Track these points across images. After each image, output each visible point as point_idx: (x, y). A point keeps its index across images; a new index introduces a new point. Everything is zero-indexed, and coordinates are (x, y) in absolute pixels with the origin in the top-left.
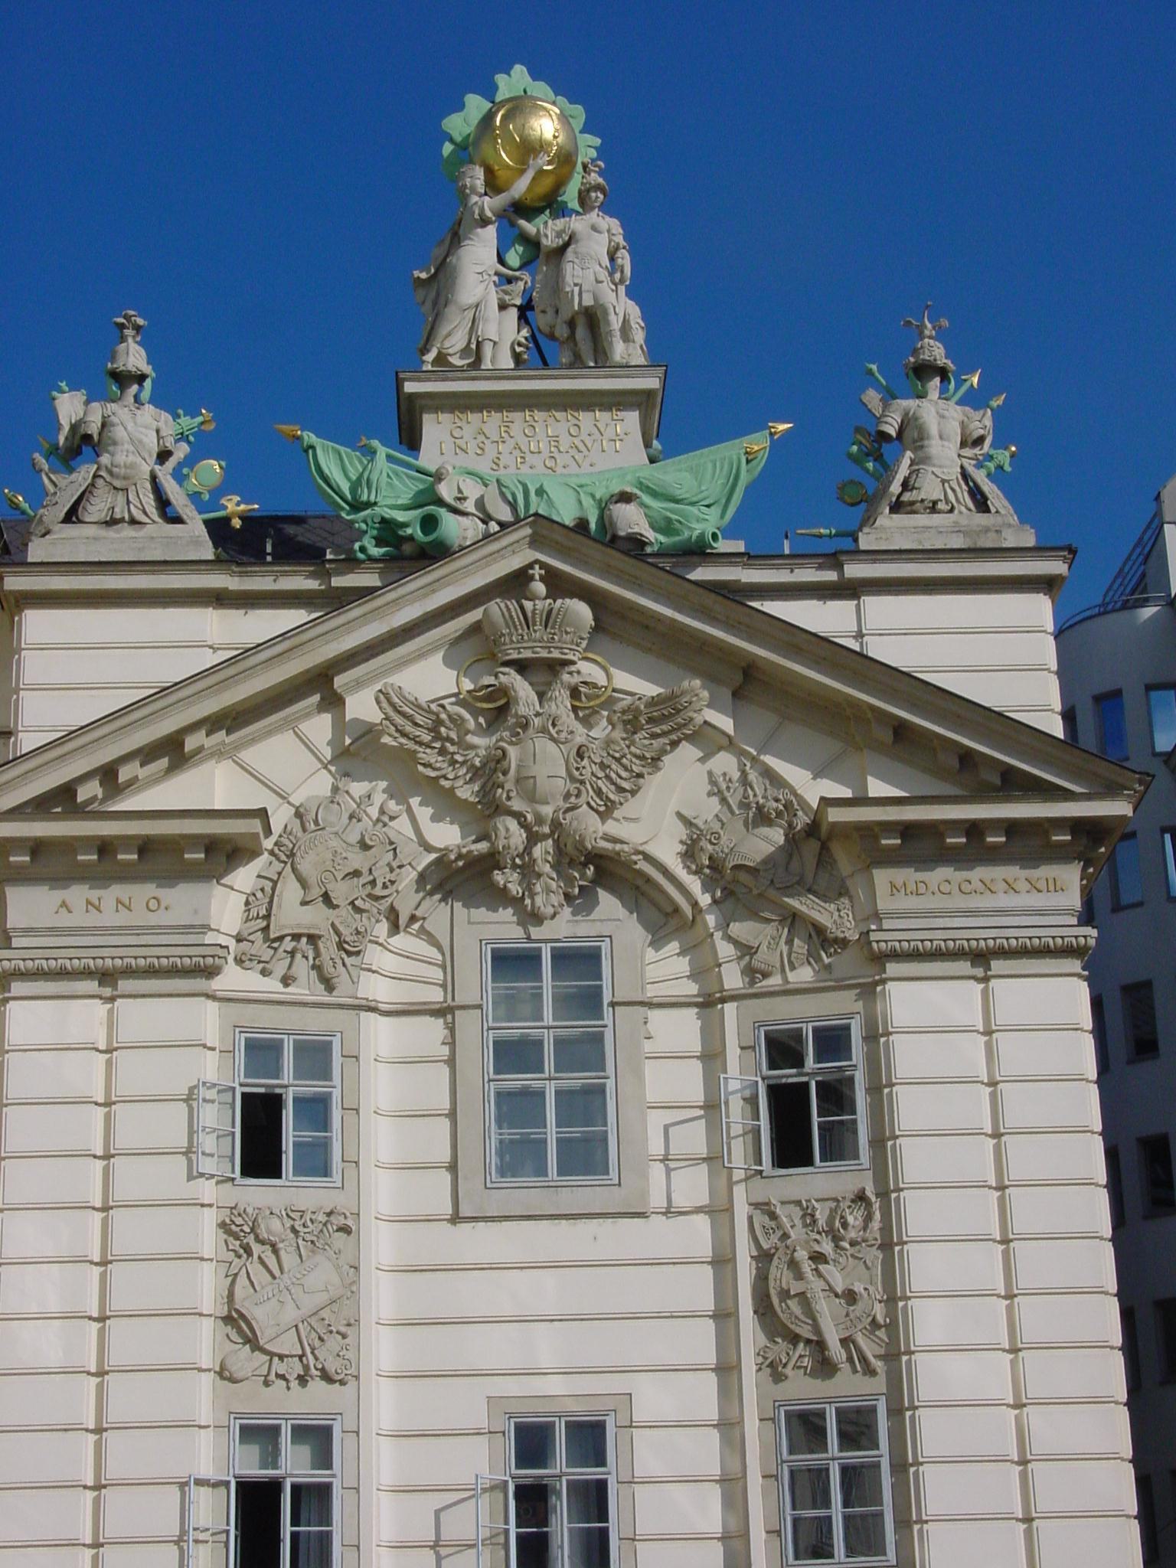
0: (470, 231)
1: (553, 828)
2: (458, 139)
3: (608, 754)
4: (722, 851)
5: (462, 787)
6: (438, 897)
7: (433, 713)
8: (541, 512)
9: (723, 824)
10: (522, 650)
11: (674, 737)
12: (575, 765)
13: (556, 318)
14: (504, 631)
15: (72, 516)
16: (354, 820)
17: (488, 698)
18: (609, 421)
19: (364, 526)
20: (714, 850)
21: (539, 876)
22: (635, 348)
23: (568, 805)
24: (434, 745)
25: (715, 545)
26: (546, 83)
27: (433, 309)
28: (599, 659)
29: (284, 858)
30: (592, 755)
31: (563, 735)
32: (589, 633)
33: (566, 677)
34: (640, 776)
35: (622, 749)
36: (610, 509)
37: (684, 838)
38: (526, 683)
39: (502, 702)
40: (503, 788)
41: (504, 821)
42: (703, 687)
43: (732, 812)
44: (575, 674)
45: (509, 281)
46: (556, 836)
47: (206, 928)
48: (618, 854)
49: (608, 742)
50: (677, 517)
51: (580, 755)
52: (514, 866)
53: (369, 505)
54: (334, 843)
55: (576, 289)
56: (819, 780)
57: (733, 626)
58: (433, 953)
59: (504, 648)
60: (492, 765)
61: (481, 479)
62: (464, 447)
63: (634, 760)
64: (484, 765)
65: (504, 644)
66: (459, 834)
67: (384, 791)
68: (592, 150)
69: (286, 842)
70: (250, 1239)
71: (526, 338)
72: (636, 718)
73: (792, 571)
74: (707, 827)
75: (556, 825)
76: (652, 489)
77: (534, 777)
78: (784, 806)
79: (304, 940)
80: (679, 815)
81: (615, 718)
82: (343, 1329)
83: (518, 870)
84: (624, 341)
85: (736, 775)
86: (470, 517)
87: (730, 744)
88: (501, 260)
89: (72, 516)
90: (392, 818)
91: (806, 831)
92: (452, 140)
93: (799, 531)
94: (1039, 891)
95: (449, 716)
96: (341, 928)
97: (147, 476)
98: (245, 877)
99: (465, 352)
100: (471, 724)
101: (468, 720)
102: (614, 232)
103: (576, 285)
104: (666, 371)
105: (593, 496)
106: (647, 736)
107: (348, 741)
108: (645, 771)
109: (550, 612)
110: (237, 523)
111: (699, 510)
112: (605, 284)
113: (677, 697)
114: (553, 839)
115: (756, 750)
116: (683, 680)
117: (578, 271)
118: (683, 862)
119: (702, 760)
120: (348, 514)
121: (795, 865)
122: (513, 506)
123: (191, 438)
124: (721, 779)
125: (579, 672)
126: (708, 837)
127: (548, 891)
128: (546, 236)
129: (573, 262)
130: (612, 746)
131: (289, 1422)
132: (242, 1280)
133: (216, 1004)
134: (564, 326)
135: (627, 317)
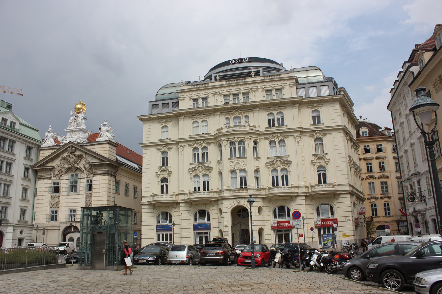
15: (45, 143)
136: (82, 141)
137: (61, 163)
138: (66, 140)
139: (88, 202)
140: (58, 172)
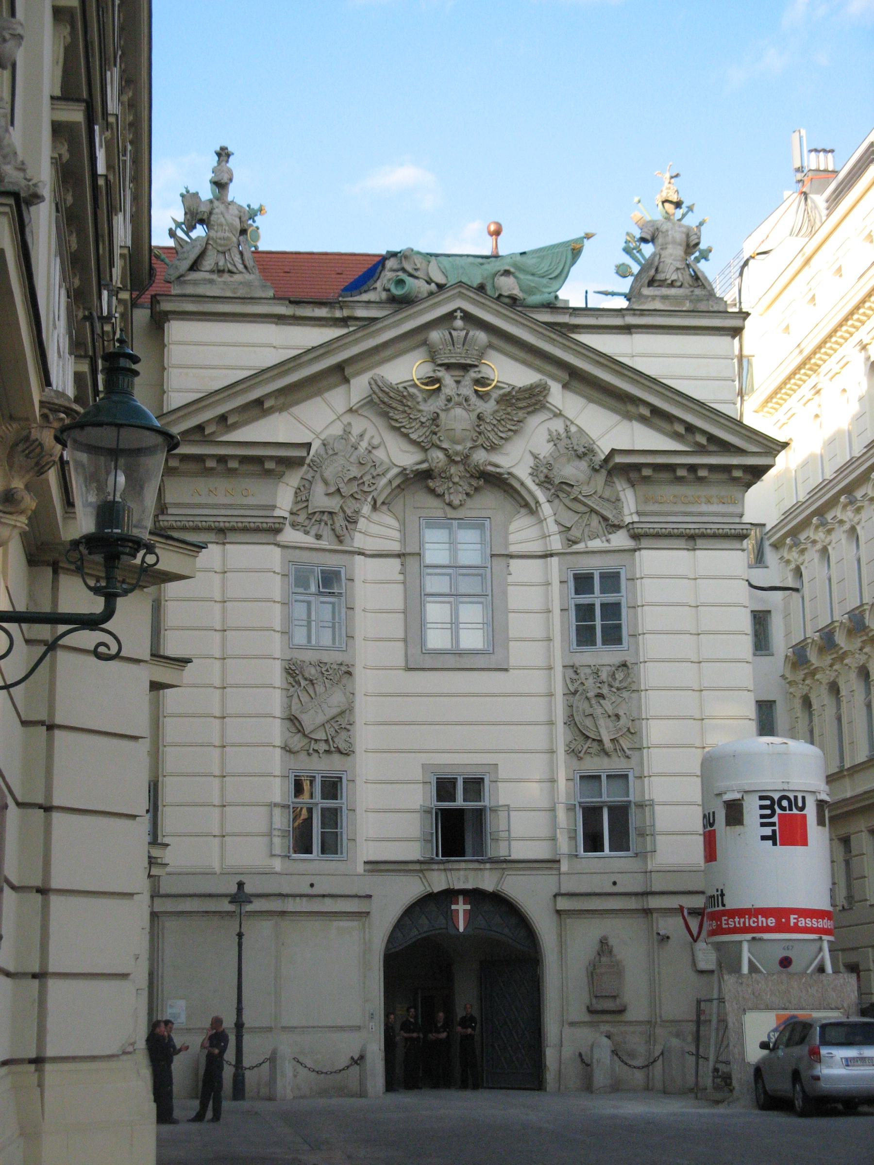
33: (473, 374)
39: (437, 386)
47: (274, 507)
48: (497, 473)
58: (395, 523)
60: (431, 422)
65: (440, 354)
70: (300, 678)
79: (326, 514)
82: (348, 727)
89: (195, 266)
94: (724, 503)
96: (346, 509)
98: (293, 479)
100: (420, 399)
131: (320, 775)
132: (295, 700)
133: (279, 549)
136: (530, 291)
137: (356, 431)
138: (404, 270)
139: (602, 722)
140: (328, 495)
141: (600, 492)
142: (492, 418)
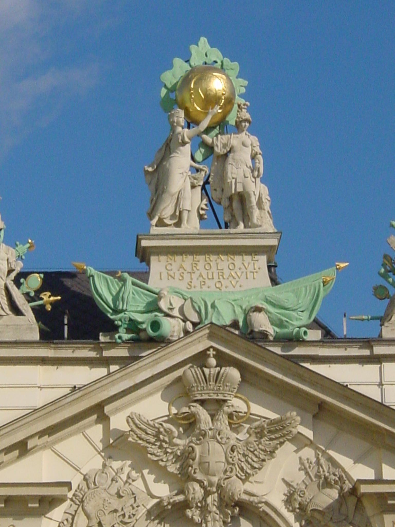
0: (177, 148)
1: (218, 488)
2: (169, 86)
3: (248, 449)
4: (306, 501)
5: (170, 465)
6: (157, 521)
7: (156, 428)
8: (214, 321)
9: (307, 486)
10: (203, 395)
11: (281, 440)
12: (230, 455)
13: (223, 194)
14: (194, 385)
16: (114, 482)
17: (184, 419)
18: (250, 261)
19: (120, 323)
20: (301, 500)
21: (210, 512)
22: (265, 213)
23: (226, 477)
24: (156, 444)
25: (305, 337)
26: (218, 49)
27: (156, 193)
28: (243, 397)
29: (78, 503)
30: (239, 450)
31: (224, 440)
32: (239, 384)
33: (226, 408)
34: (264, 460)
35: (255, 446)
36: (250, 316)
37: (286, 492)
38: (205, 411)
39: (191, 421)
40: (192, 467)
41: (192, 485)
42: (298, 415)
43: (312, 480)
44: (231, 407)
45: (198, 170)
46: (219, 492)
49: (247, 443)
50: (286, 319)
51: (232, 450)
52: (197, 507)
53: (122, 311)
54: (105, 495)
55: (234, 181)
56: (357, 464)
57: (314, 385)
59: (194, 393)
60: (187, 454)
61: (182, 295)
62: (173, 275)
63: (261, 452)
64: (182, 454)
65: (194, 391)
66: (168, 489)
67: (129, 466)
68: (243, 88)
69: (79, 494)
71: (206, 205)
72: (262, 431)
73: (346, 349)
74: (298, 487)
75: (219, 486)
76: (273, 303)
77: (209, 462)
78: (339, 478)
80: (283, 479)
81: (251, 431)
83: (199, 509)
84: (259, 209)
85: (314, 460)
86: (176, 319)
87: (311, 444)
88: (193, 158)
90: (133, 481)
91: (349, 492)
92: (165, 86)
93: (351, 318)
95: (165, 430)
97: (3, 287)
99: (173, 216)
100: (176, 434)
101: (175, 432)
102: (254, 145)
103: (233, 178)
104: (281, 236)
105: (241, 307)
106: (268, 439)
107: (111, 441)
108: (266, 458)
109: (219, 373)
110: (49, 308)
111: (298, 314)
112: (249, 178)
113: (284, 420)
114: (218, 494)
115: (324, 447)
116: (287, 412)
117: (235, 170)
118: (285, 505)
119: (296, 451)
120: (112, 315)
121: (343, 510)
122: (199, 313)
123: (24, 257)
124: (306, 461)
125: (232, 406)
126: (299, 493)
127: (214, 520)
128: (217, 146)
129: (232, 164)
130: (250, 445)
134: (227, 200)
135: (261, 195)
141: (351, 517)
142: (245, 449)
